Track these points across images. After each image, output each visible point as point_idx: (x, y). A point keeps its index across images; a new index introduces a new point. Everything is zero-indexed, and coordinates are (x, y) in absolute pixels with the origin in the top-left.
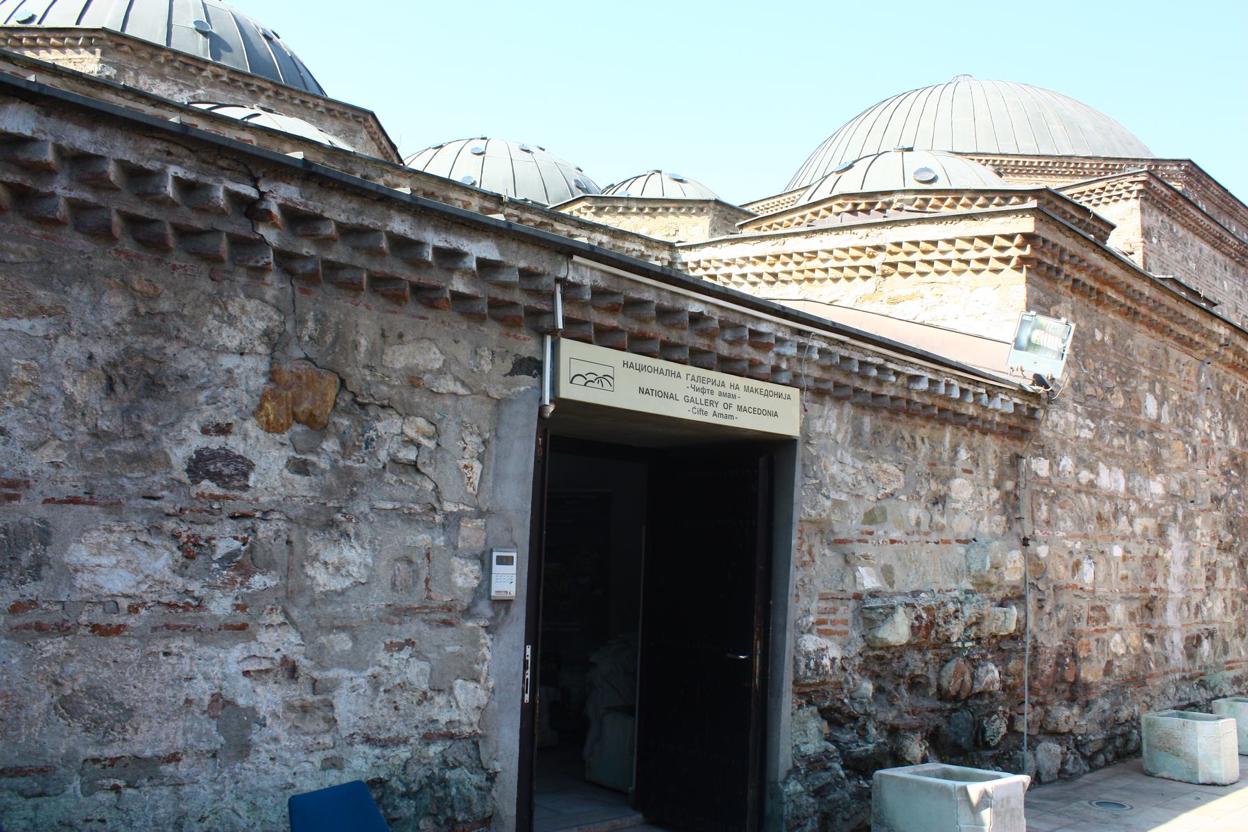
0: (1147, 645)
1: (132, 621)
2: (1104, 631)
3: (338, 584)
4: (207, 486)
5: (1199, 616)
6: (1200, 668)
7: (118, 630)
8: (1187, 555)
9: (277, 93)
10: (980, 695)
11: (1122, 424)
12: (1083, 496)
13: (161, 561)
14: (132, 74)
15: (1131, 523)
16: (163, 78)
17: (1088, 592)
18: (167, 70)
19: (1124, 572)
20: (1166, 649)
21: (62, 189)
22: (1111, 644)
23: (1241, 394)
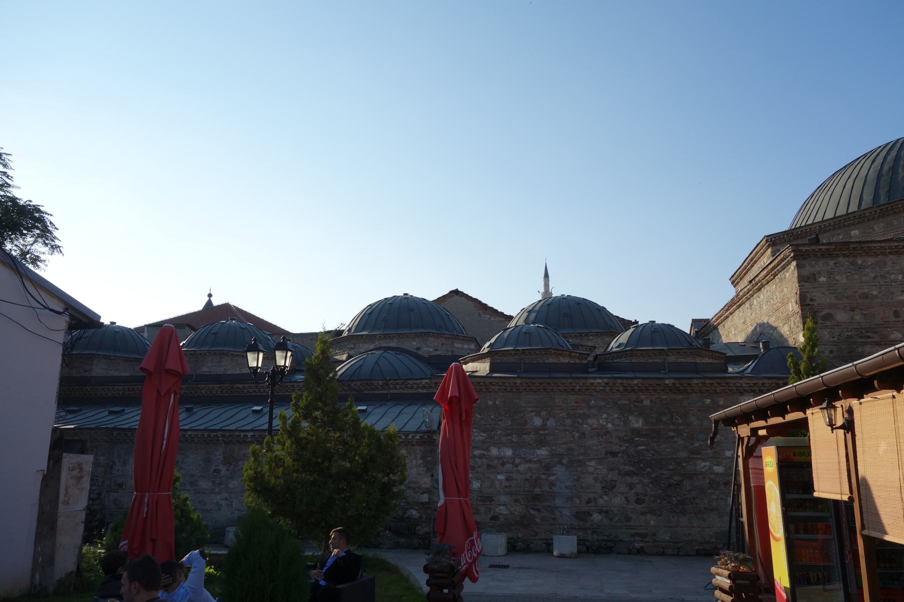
0: (532, 512)
1: (206, 492)
2: (491, 505)
3: (233, 487)
4: (215, 474)
5: (593, 504)
6: (590, 525)
7: (205, 493)
8: (575, 477)
9: (399, 336)
10: (409, 518)
11: (510, 431)
12: (477, 459)
13: (210, 484)
14: (357, 345)
15: (517, 466)
16: (366, 343)
17: (476, 491)
18: (367, 340)
19: (508, 484)
20: (555, 515)
21: (196, 439)
22: (497, 510)
23: (651, 401)
